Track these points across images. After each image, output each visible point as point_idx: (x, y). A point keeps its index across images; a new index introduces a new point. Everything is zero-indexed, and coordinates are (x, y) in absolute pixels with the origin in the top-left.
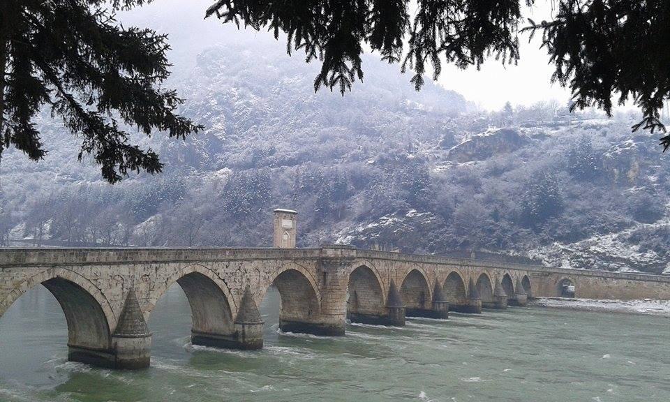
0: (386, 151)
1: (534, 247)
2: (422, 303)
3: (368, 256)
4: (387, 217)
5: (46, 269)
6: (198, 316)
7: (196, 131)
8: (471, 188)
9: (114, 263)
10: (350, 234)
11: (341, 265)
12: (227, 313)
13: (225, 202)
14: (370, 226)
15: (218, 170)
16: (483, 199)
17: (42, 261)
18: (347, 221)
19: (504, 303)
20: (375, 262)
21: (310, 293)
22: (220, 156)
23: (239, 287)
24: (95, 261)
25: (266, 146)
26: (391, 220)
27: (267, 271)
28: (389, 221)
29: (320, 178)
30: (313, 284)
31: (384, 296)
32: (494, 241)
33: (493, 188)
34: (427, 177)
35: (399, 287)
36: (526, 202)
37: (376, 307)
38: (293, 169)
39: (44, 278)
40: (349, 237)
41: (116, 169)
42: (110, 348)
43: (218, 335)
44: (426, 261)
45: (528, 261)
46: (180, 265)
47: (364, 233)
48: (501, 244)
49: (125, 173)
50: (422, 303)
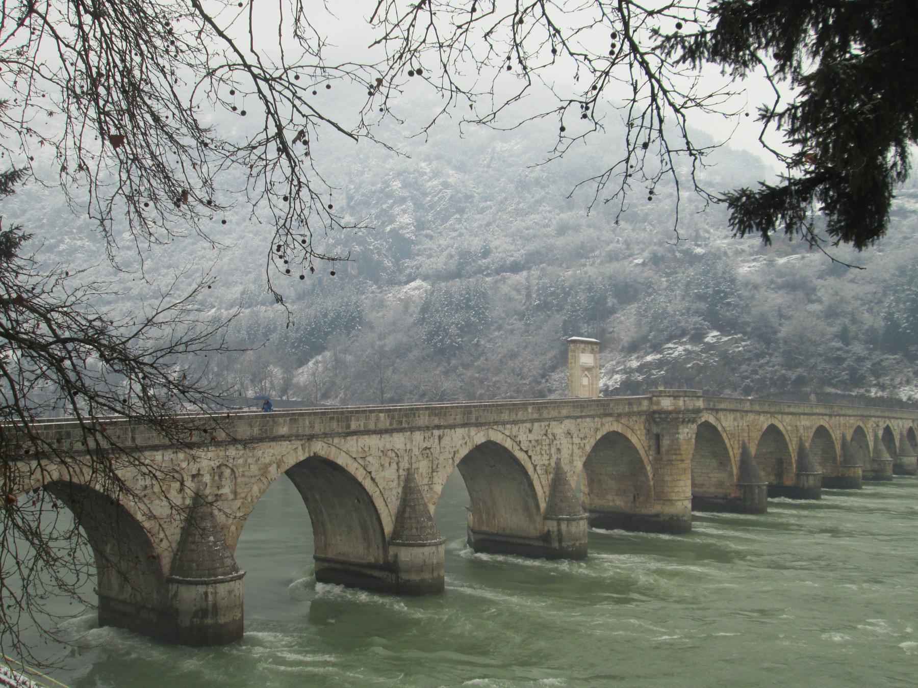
0: (660, 244)
1: (908, 382)
2: (780, 475)
3: (711, 406)
4: (675, 343)
5: (299, 443)
8: (800, 294)
10: (617, 373)
11: (683, 422)
12: (531, 504)
13: (422, 332)
14: (649, 358)
15: (407, 283)
16: (822, 312)
17: (294, 432)
18: (611, 351)
20: (721, 415)
21: (637, 466)
22: (408, 262)
23: (546, 462)
24: (362, 428)
25: (476, 244)
26: (681, 348)
27: (582, 436)
28: (677, 350)
29: (563, 288)
30: (642, 452)
31: (734, 468)
32: (844, 375)
33: (836, 293)
34: (733, 281)
36: (892, 314)
37: (720, 484)
38: (520, 277)
39: (297, 457)
40: (617, 377)
44: (787, 410)
45: (900, 404)
46: (469, 430)
47: (640, 369)
48: (856, 380)
50: (780, 475)
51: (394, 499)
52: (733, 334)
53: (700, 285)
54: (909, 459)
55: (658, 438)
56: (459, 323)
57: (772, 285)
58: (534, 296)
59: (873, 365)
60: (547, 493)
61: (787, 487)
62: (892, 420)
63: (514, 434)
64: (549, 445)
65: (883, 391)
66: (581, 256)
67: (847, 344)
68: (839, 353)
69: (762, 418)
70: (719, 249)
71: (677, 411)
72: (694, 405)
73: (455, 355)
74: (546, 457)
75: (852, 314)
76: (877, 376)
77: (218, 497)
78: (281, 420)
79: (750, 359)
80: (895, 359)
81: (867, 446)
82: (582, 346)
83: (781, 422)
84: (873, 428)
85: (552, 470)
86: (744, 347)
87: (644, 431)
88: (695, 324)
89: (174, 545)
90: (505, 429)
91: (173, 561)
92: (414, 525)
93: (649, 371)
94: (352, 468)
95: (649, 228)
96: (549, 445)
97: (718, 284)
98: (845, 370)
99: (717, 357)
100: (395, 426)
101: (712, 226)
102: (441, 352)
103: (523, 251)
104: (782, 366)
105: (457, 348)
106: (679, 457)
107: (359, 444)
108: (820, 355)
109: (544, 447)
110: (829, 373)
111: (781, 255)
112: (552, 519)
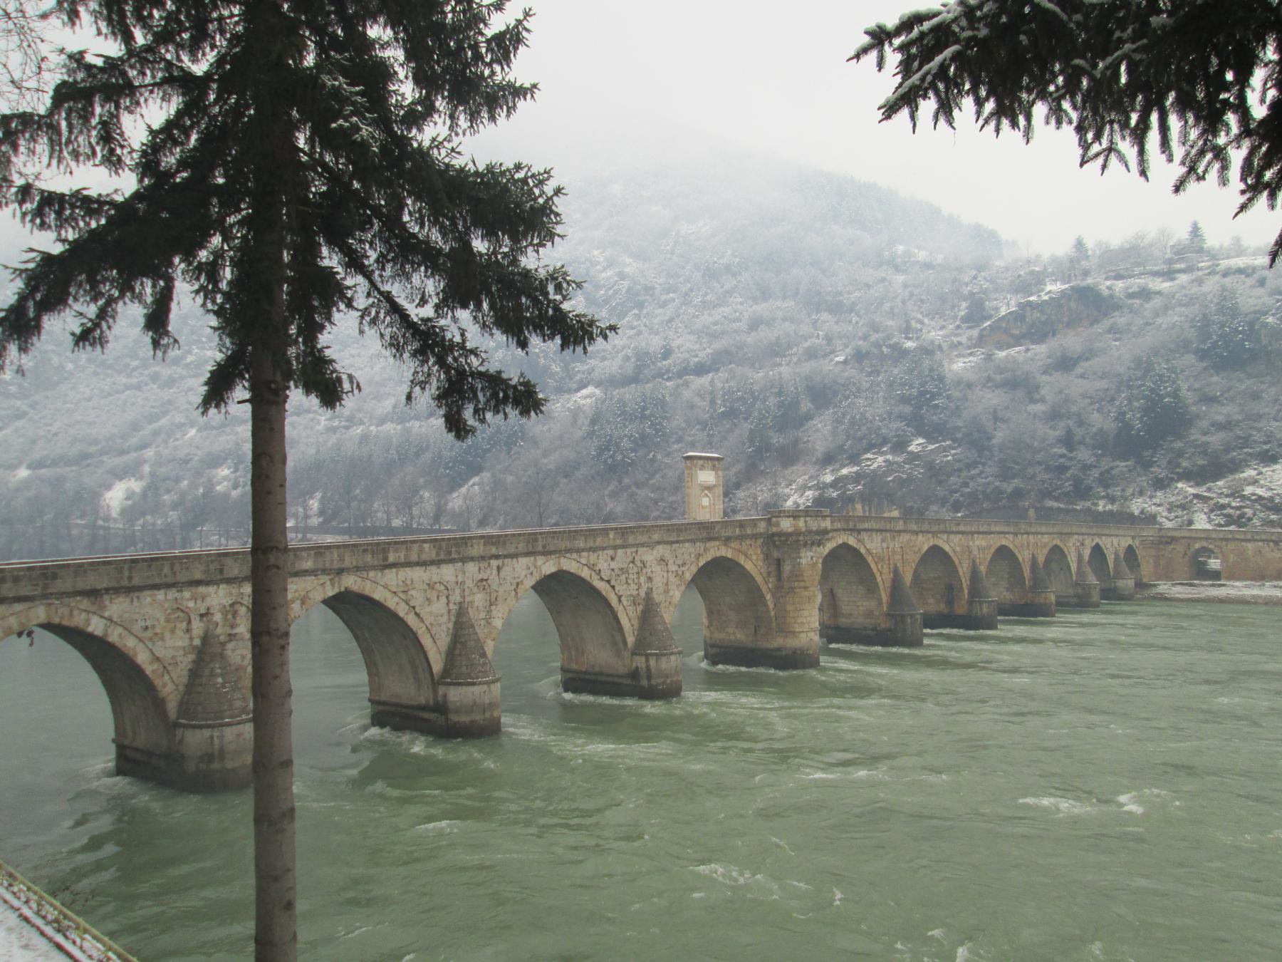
0: (865, 338)
1: (1141, 493)
2: (950, 603)
3: (851, 526)
4: (874, 454)
6: (569, 644)
7: (605, 337)
8: (1020, 393)
9: (432, 563)
10: (810, 488)
11: (805, 544)
12: (619, 639)
14: (845, 471)
15: (578, 390)
16: (1044, 412)
17: (320, 566)
18: (804, 465)
19: (1095, 596)
20: (864, 536)
21: (755, 594)
23: (635, 593)
25: (655, 343)
26: (881, 459)
28: (877, 461)
29: (752, 393)
30: (759, 580)
32: (1068, 486)
33: (1061, 392)
34: (941, 379)
35: (908, 577)
36: (1123, 414)
37: (869, 614)
38: (704, 381)
39: (325, 593)
40: (809, 493)
41: (468, 413)
42: (436, 703)
43: (608, 675)
45: (1131, 519)
47: (834, 485)
48: (1082, 492)
49: (483, 421)
50: (950, 603)
51: (443, 636)
52: (941, 441)
53: (906, 385)
54: (1125, 581)
55: (779, 562)
56: (632, 436)
57: (988, 383)
58: (719, 402)
59: (1102, 474)
60: (636, 626)
61: (959, 616)
62: (1103, 538)
63: (592, 562)
64: (638, 573)
65: (1112, 504)
66: (777, 355)
67: (1071, 451)
68: (1062, 460)
69: (920, 538)
70: (932, 342)
71: (797, 533)
72: (819, 526)
73: (627, 473)
74: (633, 586)
75: (1079, 415)
76: (1106, 486)
77: (232, 637)
78: (304, 554)
79: (960, 470)
80: (1126, 466)
81: (1069, 568)
82: (701, 462)
83: (947, 542)
84: (1077, 548)
85: (641, 601)
86: (953, 455)
87: (761, 556)
88: (897, 429)
89: (181, 688)
90: (580, 557)
91: (180, 704)
92: (464, 663)
93: (845, 486)
94: (391, 602)
95: (855, 319)
96: (638, 573)
97: (922, 385)
98: (1068, 480)
99: (923, 468)
100: (442, 557)
101: (927, 315)
102: (612, 469)
103: (709, 351)
104: (997, 477)
105: (629, 465)
106: (802, 584)
107: (400, 577)
108: (1039, 463)
109: (631, 576)
110: (1050, 484)
111: (1001, 349)
112: (640, 655)
